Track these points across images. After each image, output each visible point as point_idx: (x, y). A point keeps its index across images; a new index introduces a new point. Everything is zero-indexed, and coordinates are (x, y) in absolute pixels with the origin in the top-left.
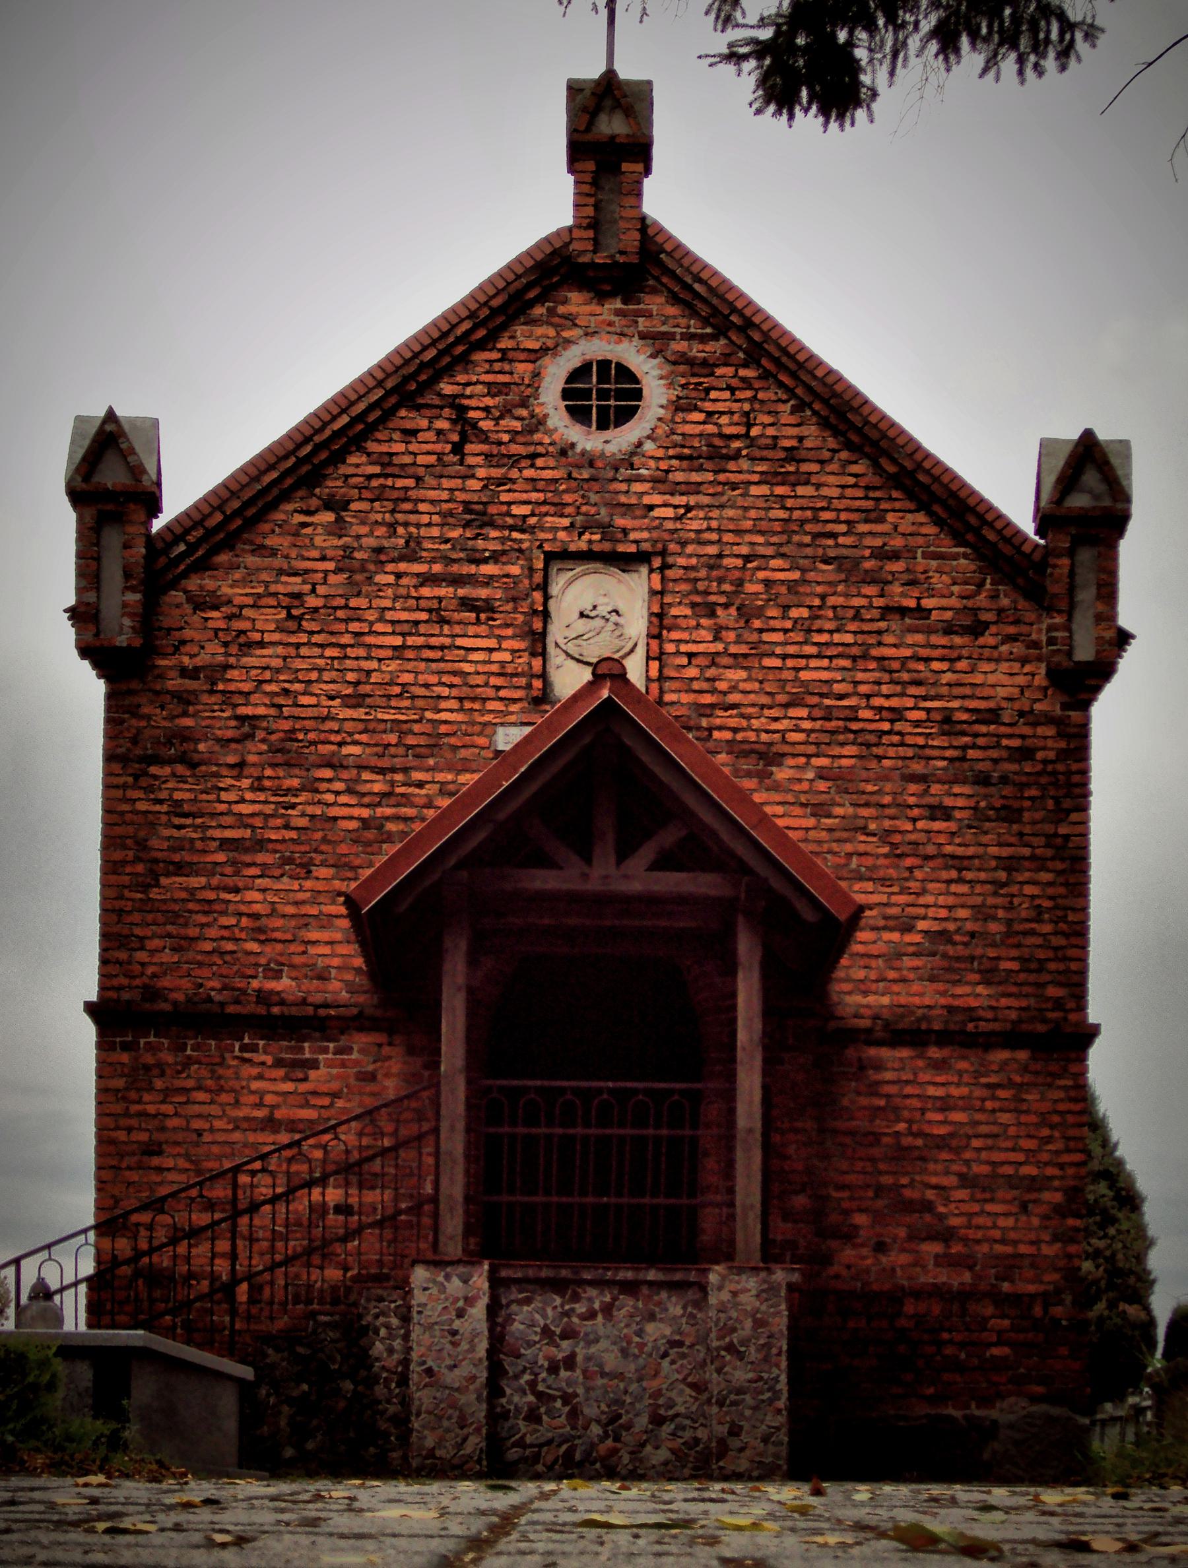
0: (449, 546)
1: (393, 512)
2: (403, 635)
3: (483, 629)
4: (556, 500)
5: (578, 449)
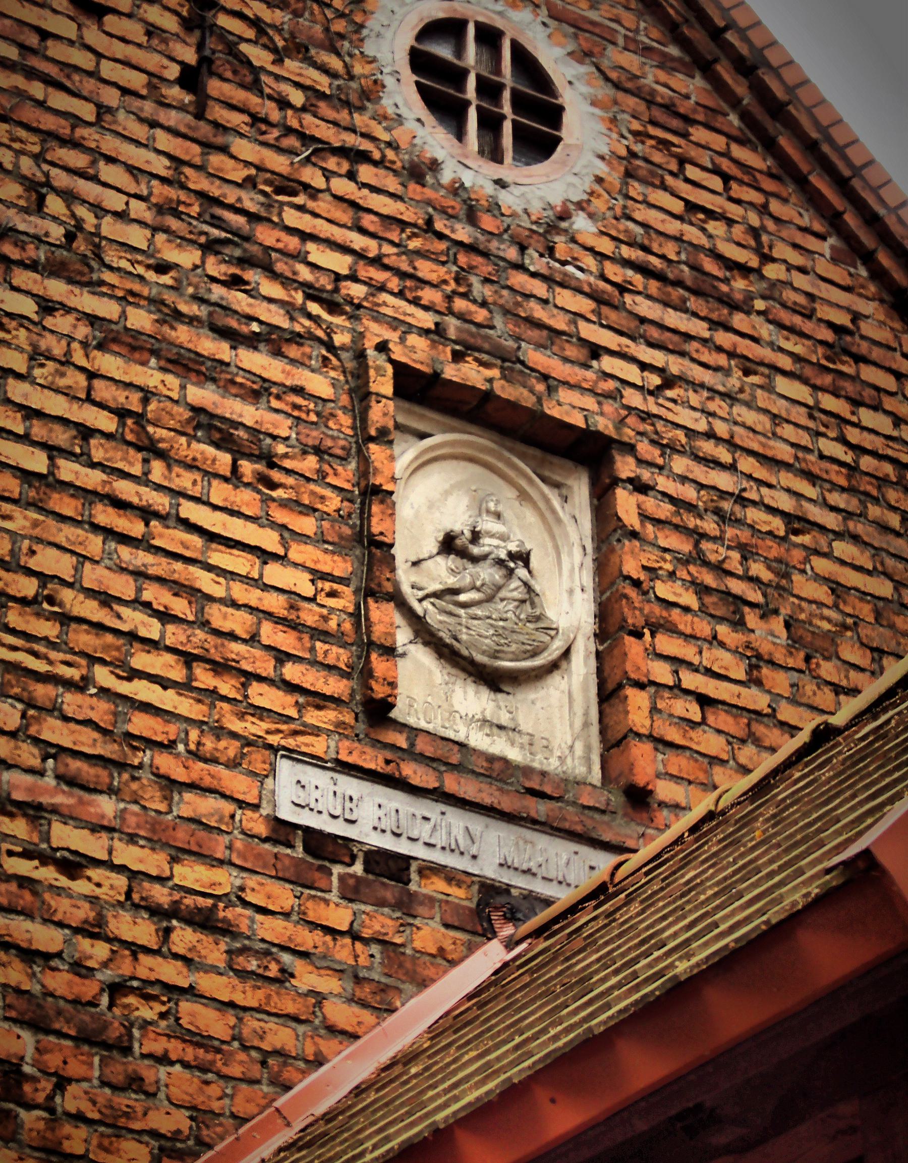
0: (166, 279)
1: (38, 158)
2: (53, 451)
3: (246, 500)
4: (405, 267)
5: (446, 177)
